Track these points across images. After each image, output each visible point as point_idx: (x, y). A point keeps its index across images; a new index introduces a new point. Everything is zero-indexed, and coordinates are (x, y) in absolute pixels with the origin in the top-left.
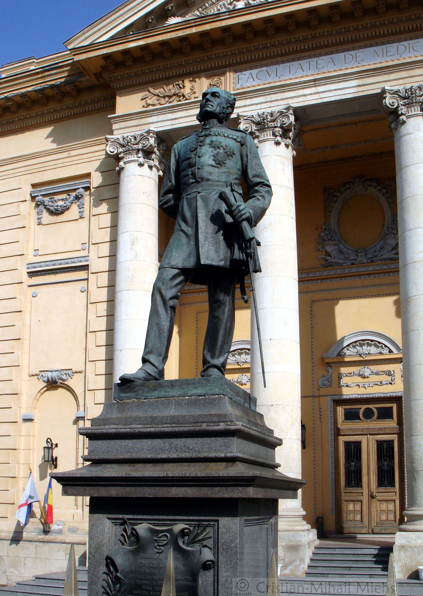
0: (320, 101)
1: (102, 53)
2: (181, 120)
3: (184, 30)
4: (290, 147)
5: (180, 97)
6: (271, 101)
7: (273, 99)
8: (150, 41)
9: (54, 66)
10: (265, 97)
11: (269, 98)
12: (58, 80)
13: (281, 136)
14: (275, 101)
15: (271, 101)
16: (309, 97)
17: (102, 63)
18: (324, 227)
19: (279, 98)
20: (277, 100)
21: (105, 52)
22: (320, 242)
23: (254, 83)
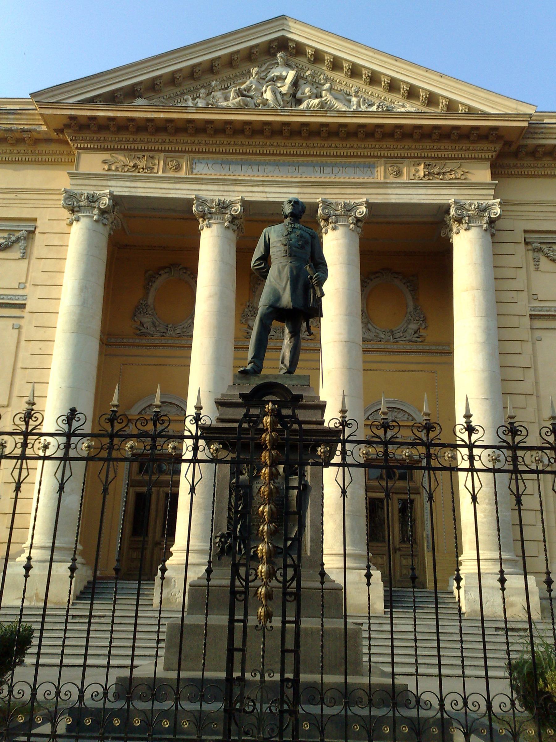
0: (265, 199)
1: (69, 114)
2: (139, 190)
3: (153, 113)
4: (236, 232)
5: (140, 169)
6: (225, 191)
7: (226, 189)
8: (119, 114)
9: (13, 111)
10: (219, 186)
11: (221, 188)
12: (15, 126)
13: (229, 222)
14: (227, 191)
15: (225, 191)
16: (257, 195)
17: (66, 121)
18: (248, 304)
19: (231, 190)
20: (230, 191)
21: (72, 114)
22: (244, 316)
23: (209, 172)
